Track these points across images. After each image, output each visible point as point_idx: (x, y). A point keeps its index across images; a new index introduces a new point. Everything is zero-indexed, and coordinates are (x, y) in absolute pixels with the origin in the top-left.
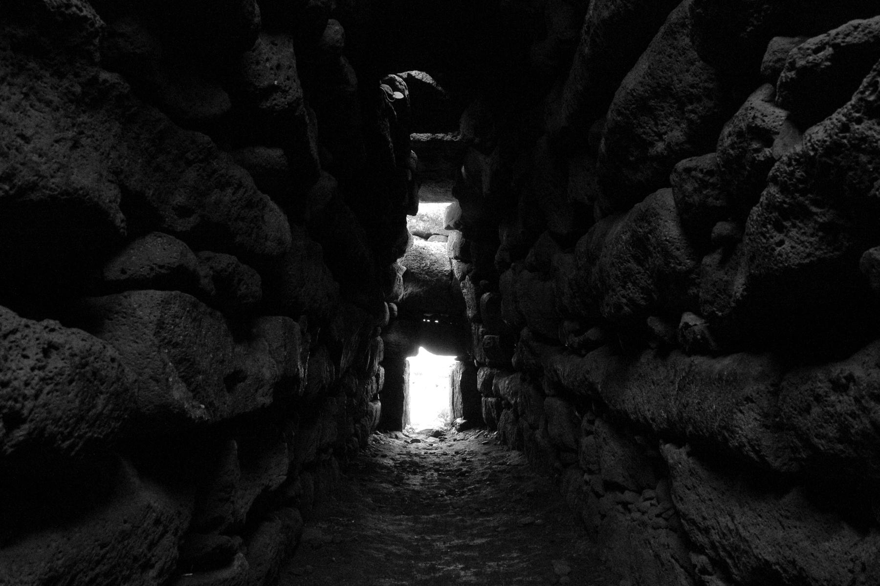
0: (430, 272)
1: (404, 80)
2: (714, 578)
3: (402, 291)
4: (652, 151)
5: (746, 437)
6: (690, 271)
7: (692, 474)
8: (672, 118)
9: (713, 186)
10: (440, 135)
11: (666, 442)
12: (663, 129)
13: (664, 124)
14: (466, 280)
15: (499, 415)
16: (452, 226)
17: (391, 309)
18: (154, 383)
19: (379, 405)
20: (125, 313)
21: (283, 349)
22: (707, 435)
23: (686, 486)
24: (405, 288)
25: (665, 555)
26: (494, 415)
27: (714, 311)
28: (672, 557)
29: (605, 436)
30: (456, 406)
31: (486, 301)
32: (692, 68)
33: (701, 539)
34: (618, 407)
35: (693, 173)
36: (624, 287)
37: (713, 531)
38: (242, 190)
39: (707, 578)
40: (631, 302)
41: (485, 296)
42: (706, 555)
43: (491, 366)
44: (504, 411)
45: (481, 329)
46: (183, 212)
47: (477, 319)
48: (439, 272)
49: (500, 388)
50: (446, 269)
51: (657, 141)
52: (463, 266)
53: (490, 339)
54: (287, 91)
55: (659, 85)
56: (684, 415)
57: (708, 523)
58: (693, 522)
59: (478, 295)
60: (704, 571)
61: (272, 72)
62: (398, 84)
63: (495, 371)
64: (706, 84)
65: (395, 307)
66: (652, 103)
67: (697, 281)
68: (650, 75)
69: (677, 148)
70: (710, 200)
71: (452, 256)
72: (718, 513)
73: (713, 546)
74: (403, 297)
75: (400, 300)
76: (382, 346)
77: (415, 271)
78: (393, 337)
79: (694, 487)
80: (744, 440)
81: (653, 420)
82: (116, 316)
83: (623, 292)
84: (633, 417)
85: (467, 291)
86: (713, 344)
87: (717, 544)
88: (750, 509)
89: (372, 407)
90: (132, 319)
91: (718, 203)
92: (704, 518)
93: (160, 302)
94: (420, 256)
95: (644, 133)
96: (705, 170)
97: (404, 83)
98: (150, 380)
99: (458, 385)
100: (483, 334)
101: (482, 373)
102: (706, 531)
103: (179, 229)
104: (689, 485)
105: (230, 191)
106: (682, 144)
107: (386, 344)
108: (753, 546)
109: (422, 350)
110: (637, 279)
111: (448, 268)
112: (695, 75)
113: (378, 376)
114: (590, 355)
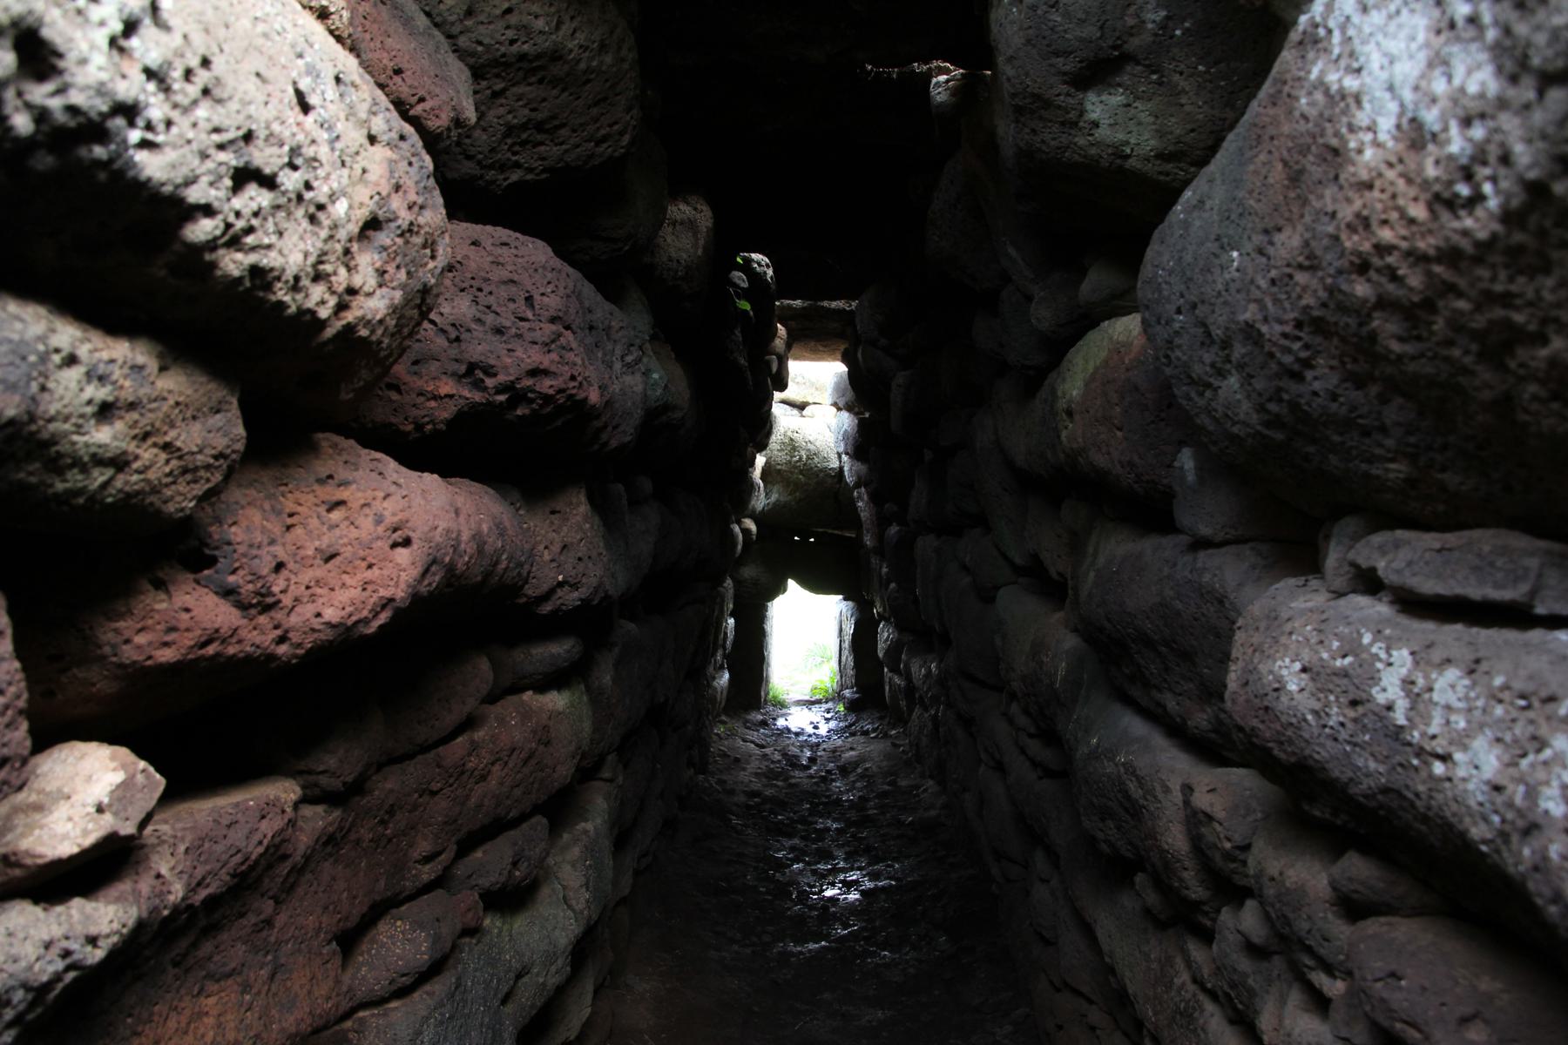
3: (760, 501)
15: (911, 711)
16: (841, 405)
17: (746, 532)
35: (1216, 825)
41: (894, 529)
43: (900, 628)
45: (885, 570)
47: (880, 551)
48: (821, 471)
59: (882, 522)
61: (554, 564)
65: (753, 527)
71: (841, 449)
78: (748, 572)
94: (792, 445)
99: (848, 638)
107: (738, 583)
109: (792, 584)
111: (835, 464)
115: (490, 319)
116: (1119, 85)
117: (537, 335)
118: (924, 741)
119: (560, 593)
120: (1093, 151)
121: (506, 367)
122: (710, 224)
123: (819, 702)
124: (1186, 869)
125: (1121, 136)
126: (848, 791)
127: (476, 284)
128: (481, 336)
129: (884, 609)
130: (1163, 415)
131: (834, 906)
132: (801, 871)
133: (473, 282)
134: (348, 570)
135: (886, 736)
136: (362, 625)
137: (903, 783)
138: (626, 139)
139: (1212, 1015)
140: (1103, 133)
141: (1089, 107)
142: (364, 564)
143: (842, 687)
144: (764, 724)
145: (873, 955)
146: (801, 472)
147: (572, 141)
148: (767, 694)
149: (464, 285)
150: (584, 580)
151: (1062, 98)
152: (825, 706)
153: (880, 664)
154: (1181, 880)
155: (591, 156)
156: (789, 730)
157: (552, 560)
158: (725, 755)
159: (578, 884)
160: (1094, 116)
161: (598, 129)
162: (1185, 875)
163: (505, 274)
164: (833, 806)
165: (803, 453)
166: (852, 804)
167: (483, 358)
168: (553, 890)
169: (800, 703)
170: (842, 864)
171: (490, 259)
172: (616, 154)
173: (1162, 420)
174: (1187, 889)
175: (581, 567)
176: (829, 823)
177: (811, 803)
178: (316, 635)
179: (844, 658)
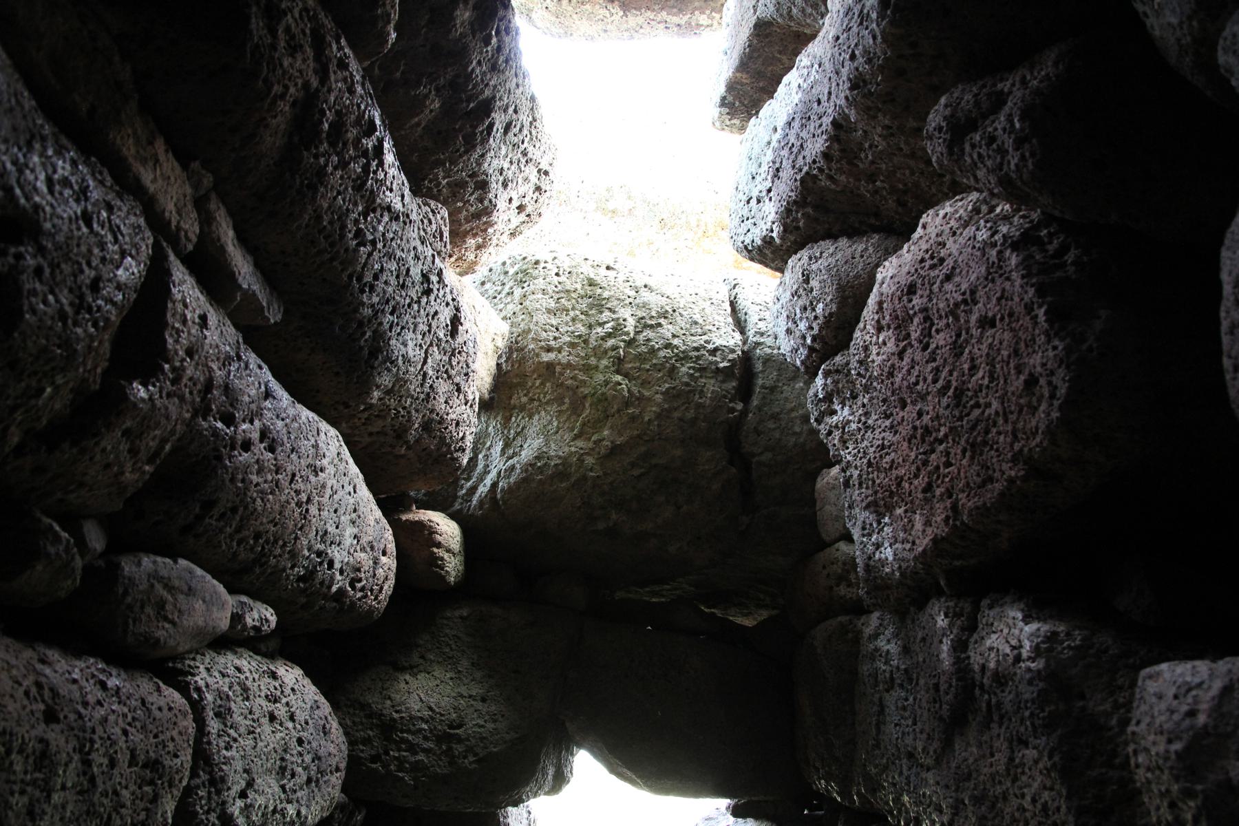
0: (640, 357)
24: (507, 445)
48: (684, 357)
50: (719, 342)
65: (447, 529)
74: (494, 485)
75: (481, 502)
77: (563, 357)
146: (619, 364)
165: (625, 313)
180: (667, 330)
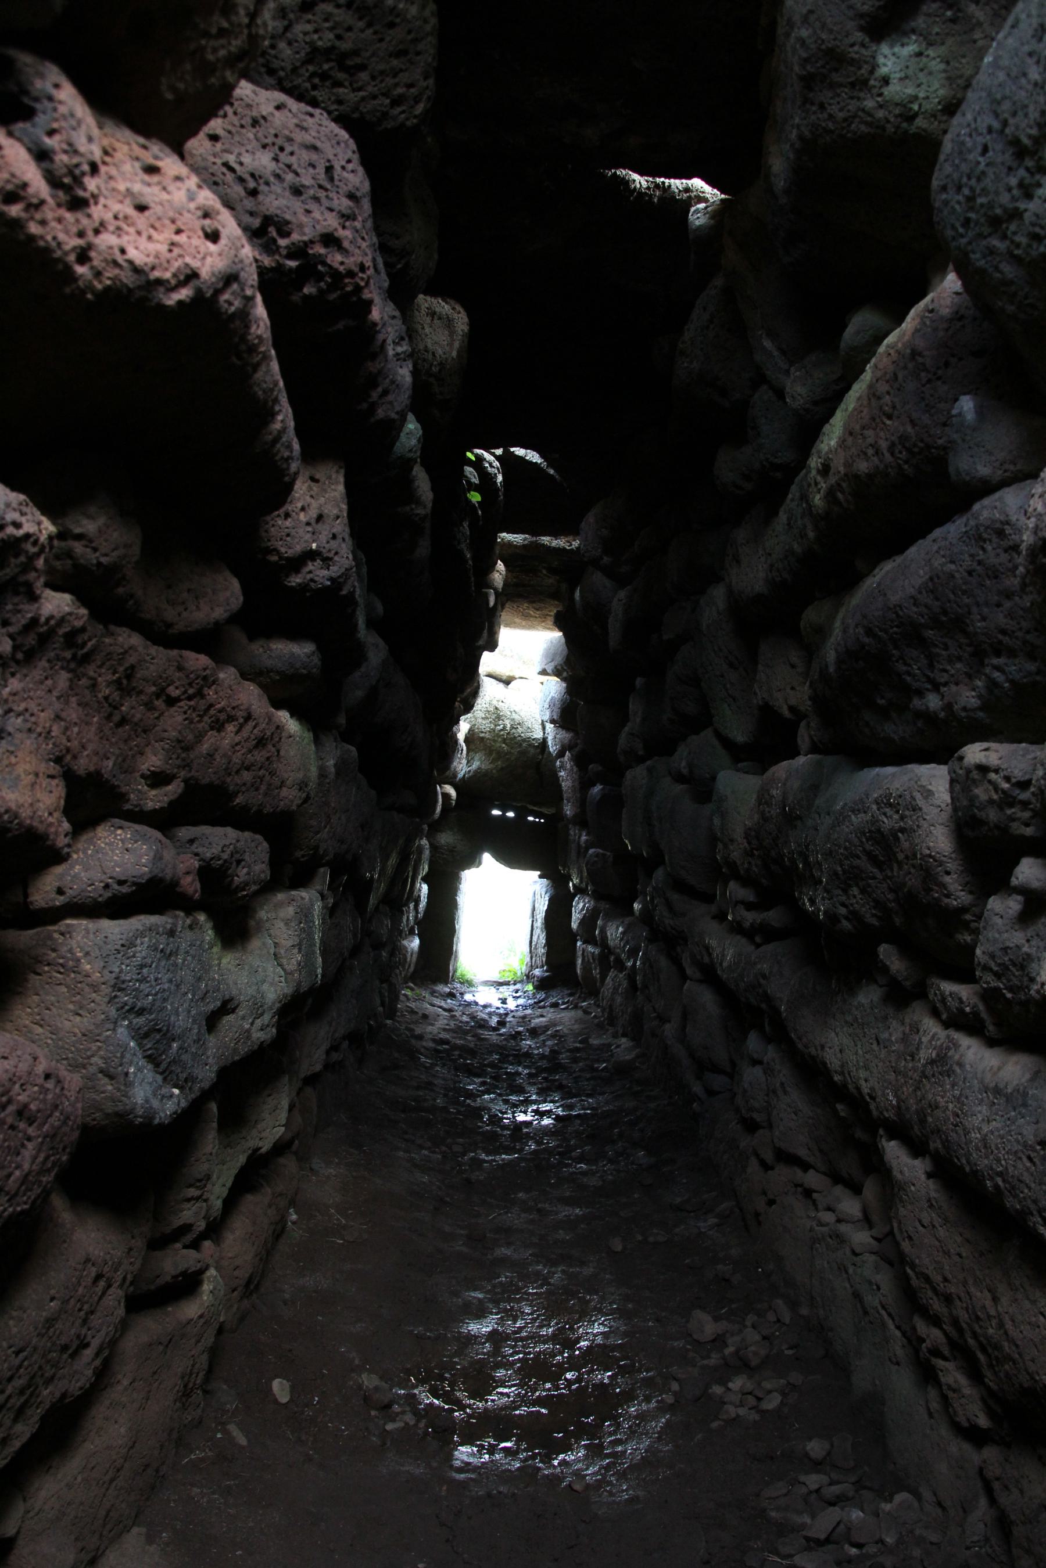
0: (511, 739)
1: (497, 458)
2: (950, 1366)
3: (462, 766)
4: (917, 703)
5: (1035, 1202)
6: (964, 910)
7: (931, 1206)
8: (959, 665)
9: (1025, 804)
10: (546, 540)
11: (891, 1138)
12: (944, 678)
13: (945, 671)
14: (566, 758)
15: (603, 977)
17: (446, 796)
18: (106, 1080)
19: (416, 942)
20: (62, 965)
21: (296, 951)
22: (967, 1169)
23: (920, 1221)
25: (872, 1300)
26: (596, 972)
27: (1000, 989)
28: (883, 1307)
29: (784, 1080)
30: (536, 948)
31: (598, 798)
32: (1008, 604)
33: (937, 1306)
34: (813, 1052)
35: (993, 776)
36: (845, 891)
37: (958, 1303)
38: (251, 724)
39: (940, 1363)
40: (854, 916)
41: (597, 789)
42: (941, 1329)
43: (597, 896)
44: (612, 973)
45: (584, 838)
46: (157, 779)
47: (581, 821)
48: (524, 740)
49: (609, 934)
50: (535, 736)
51: (927, 690)
52: (565, 736)
53: (597, 855)
54: (331, 559)
55: (945, 612)
56: (930, 1119)
57: (953, 1289)
58: (927, 1279)
59: (584, 784)
60: (936, 1352)
61: (310, 529)
62: (487, 465)
63: (604, 905)
64: (1028, 637)
65: (453, 792)
66: (929, 633)
67: (973, 925)
68: (932, 591)
69: (963, 714)
70: (1014, 825)
71: (547, 717)
72: (971, 1281)
73: (955, 1322)
76: (427, 853)
77: (487, 736)
78: (446, 838)
79: (934, 1226)
80: (1033, 1207)
81: (873, 1098)
82: (46, 968)
83: (844, 898)
84: (837, 1078)
85: (566, 775)
86: (991, 1028)
87: (964, 1326)
88: (1028, 1299)
89: (406, 948)
90: (73, 975)
91: (1029, 831)
92: (946, 1280)
93: (118, 947)
94: (497, 715)
95: (909, 674)
96: (1014, 780)
97: (496, 464)
98: (100, 1075)
99: (540, 916)
100: (589, 845)
101: (581, 905)
102: (948, 1299)
103: (150, 805)
104: (926, 1222)
105: (230, 728)
106: (974, 710)
107: (434, 848)
108: (1027, 1358)
109: (487, 858)
110: (869, 886)
111: (538, 734)
112: (1010, 615)
113: (417, 901)
114: (769, 948)
115: (290, 177)
116: (913, 31)
117: (335, 204)
118: (619, 1000)
119: (310, 566)
120: (880, 114)
121: (301, 226)
122: (466, 328)
123: (507, 983)
124: (948, 873)
125: (910, 91)
126: (538, 1048)
127: (279, 141)
128: (279, 191)
129: (581, 881)
130: (940, 372)
131: (527, 1127)
132: (492, 1100)
133: (276, 140)
134: (157, 225)
135: (576, 1007)
136: (162, 289)
137: (595, 1042)
138: (420, 109)
139: (969, 1047)
140: (895, 90)
141: (881, 60)
142: (173, 227)
143: (532, 967)
144: (452, 995)
145: (569, 1165)
146: (504, 741)
147: (370, 89)
148: (455, 971)
149: (266, 141)
150: (336, 558)
151: (856, 48)
152: (512, 988)
153: (573, 937)
154: (943, 886)
155: (385, 115)
156: (476, 1004)
157: (308, 524)
158: (413, 1012)
159: (290, 943)
160: (884, 71)
161: (396, 85)
162: (947, 879)
163: (308, 138)
164: (523, 1057)
166: (542, 1057)
167: (278, 212)
168: (264, 944)
169: (486, 983)
170: (534, 1097)
171: (295, 121)
172: (409, 123)
173: (939, 378)
174: (948, 896)
175: (334, 544)
176: (520, 1069)
177: (501, 1054)
178: (117, 271)
179: (535, 938)
180: (520, 730)
